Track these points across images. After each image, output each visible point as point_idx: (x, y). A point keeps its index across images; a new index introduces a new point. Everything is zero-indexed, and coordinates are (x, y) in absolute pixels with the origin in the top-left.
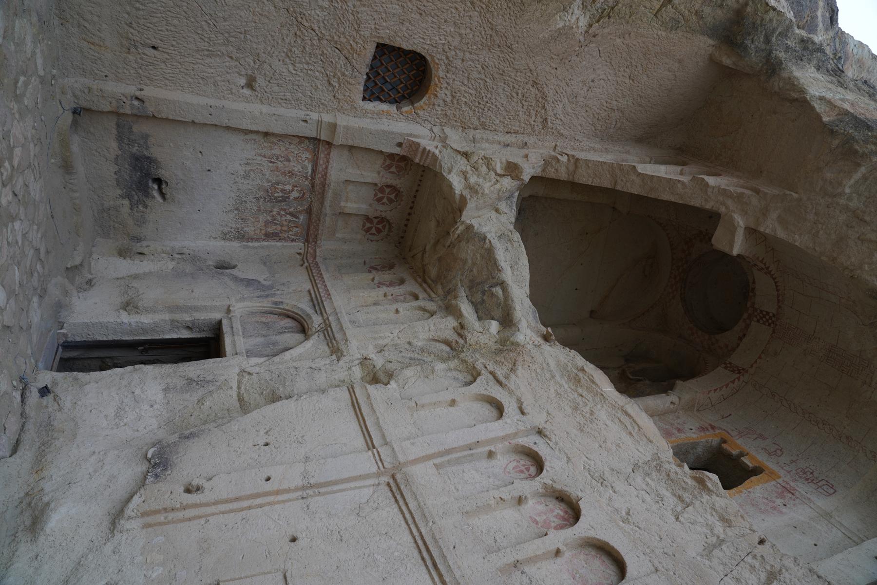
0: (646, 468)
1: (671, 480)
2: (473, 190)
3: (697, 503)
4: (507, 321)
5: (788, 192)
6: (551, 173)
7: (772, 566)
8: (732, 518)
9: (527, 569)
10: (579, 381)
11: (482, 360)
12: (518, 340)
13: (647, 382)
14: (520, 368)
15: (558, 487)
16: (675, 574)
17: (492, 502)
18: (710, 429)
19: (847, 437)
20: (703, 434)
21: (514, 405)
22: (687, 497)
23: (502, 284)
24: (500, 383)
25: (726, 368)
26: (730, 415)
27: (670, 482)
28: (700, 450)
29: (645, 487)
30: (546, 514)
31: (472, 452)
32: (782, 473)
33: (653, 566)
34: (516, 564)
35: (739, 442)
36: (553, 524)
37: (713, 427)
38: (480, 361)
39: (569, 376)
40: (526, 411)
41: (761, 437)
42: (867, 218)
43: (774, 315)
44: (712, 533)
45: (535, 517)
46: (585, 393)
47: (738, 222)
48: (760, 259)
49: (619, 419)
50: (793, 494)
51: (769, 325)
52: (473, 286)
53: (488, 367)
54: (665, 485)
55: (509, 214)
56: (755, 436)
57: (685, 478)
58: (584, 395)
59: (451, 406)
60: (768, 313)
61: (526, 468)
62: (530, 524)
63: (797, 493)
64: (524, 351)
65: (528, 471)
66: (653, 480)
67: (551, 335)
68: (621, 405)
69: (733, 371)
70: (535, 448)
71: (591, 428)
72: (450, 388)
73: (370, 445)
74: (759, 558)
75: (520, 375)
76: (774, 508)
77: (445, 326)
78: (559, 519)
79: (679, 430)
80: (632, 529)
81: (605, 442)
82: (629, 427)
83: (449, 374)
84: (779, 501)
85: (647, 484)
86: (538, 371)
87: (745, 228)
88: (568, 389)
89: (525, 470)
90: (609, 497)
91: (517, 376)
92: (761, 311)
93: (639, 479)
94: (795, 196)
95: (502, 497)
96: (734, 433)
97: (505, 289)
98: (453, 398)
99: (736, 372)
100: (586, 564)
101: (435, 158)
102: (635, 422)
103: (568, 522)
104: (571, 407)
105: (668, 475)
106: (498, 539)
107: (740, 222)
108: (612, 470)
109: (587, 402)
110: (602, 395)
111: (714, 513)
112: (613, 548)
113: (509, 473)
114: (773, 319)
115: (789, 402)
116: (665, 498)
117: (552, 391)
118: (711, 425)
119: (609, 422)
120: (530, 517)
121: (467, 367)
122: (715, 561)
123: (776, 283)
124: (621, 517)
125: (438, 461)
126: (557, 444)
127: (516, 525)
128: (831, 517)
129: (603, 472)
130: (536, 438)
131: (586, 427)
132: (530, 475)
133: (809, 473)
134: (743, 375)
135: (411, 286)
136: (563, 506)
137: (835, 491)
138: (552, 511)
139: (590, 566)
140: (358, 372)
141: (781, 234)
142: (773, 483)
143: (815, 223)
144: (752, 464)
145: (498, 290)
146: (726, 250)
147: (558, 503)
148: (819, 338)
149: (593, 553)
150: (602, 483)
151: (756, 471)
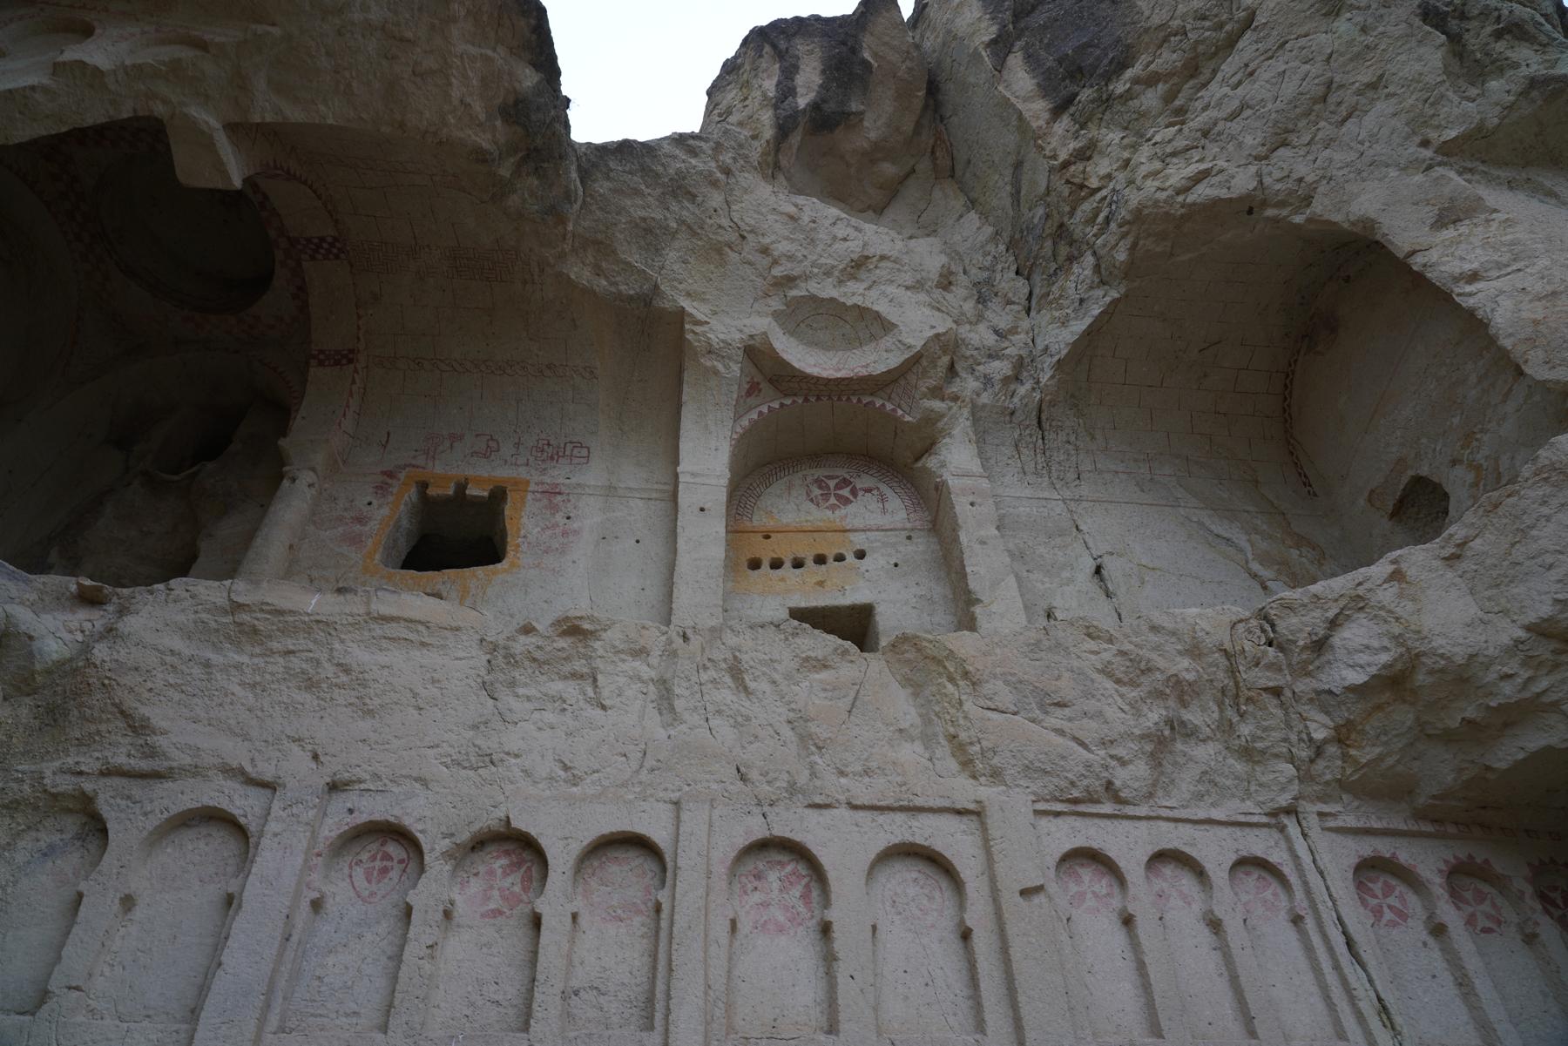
0: (501, 677)
1: (544, 663)
3: (599, 663)
5: (260, 29)
7: (725, 660)
8: (642, 642)
9: (575, 983)
10: (255, 631)
11: (48, 768)
12: (55, 657)
13: (210, 466)
14: (145, 711)
15: (464, 836)
16: (689, 785)
17: (427, 967)
18: (390, 481)
19: (549, 367)
20: (391, 499)
21: (232, 786)
22: (579, 665)
24: (157, 776)
25: (321, 364)
26: (388, 434)
27: (546, 667)
28: (405, 523)
29: (528, 706)
30: (491, 888)
31: (294, 939)
32: (523, 473)
33: (665, 802)
35: (439, 469)
36: (517, 889)
37: (390, 474)
38: (48, 773)
39: (228, 637)
40: (268, 777)
41: (455, 438)
42: (409, 35)
43: (336, 239)
44: (643, 682)
45: (486, 908)
46: (290, 644)
47: (207, 123)
48: (272, 164)
49: (385, 638)
50: (560, 493)
51: (337, 257)
53: (83, 768)
54: (544, 677)
56: (447, 444)
57: (555, 645)
58: (291, 647)
59: (129, 910)
60: (322, 239)
61: (382, 860)
62: (494, 925)
63: (563, 488)
64: (109, 674)
65: (390, 858)
66: (526, 685)
67: (99, 589)
68: (362, 611)
69: (337, 363)
70: (361, 818)
71: (376, 695)
72: (83, 887)
74: (709, 664)
75: (164, 724)
76: (565, 534)
78: (512, 871)
79: (360, 520)
80: (593, 783)
81: (415, 695)
82: (411, 636)
83: (20, 858)
84: (559, 518)
85: (529, 699)
86: (171, 681)
87: (223, 127)
88: (256, 660)
89: (385, 863)
90: (522, 771)
91: (164, 733)
92: (309, 240)
93: (508, 700)
94: (276, 31)
95: (431, 943)
96: (420, 461)
98: (118, 895)
99: (344, 361)
100: (607, 886)
102: (411, 621)
103: (526, 862)
104: (299, 688)
105: (535, 660)
106: (496, 998)
107: (209, 120)
108: (475, 727)
109: (311, 655)
110: (318, 622)
111: (623, 656)
112: (612, 833)
113: (373, 894)
114: (338, 245)
115: (447, 362)
116: (564, 695)
117: (237, 689)
118: (384, 473)
119: (382, 658)
120: (482, 916)
121: (36, 808)
122: (686, 716)
123: (310, 187)
124: (565, 781)
125: (273, 1021)
126: (377, 777)
127: (485, 950)
128: (615, 488)
129: (475, 746)
130: (340, 802)
131: (368, 701)
132: (401, 861)
133: (546, 447)
134: (357, 361)
136: (492, 848)
137: (588, 448)
138: (491, 873)
139: (613, 884)
141: (295, 115)
142: (530, 497)
143: (336, 72)
144: (484, 490)
146: (220, 186)
147: (481, 853)
148: (428, 246)
149: (596, 864)
150: (492, 762)
151: (498, 496)
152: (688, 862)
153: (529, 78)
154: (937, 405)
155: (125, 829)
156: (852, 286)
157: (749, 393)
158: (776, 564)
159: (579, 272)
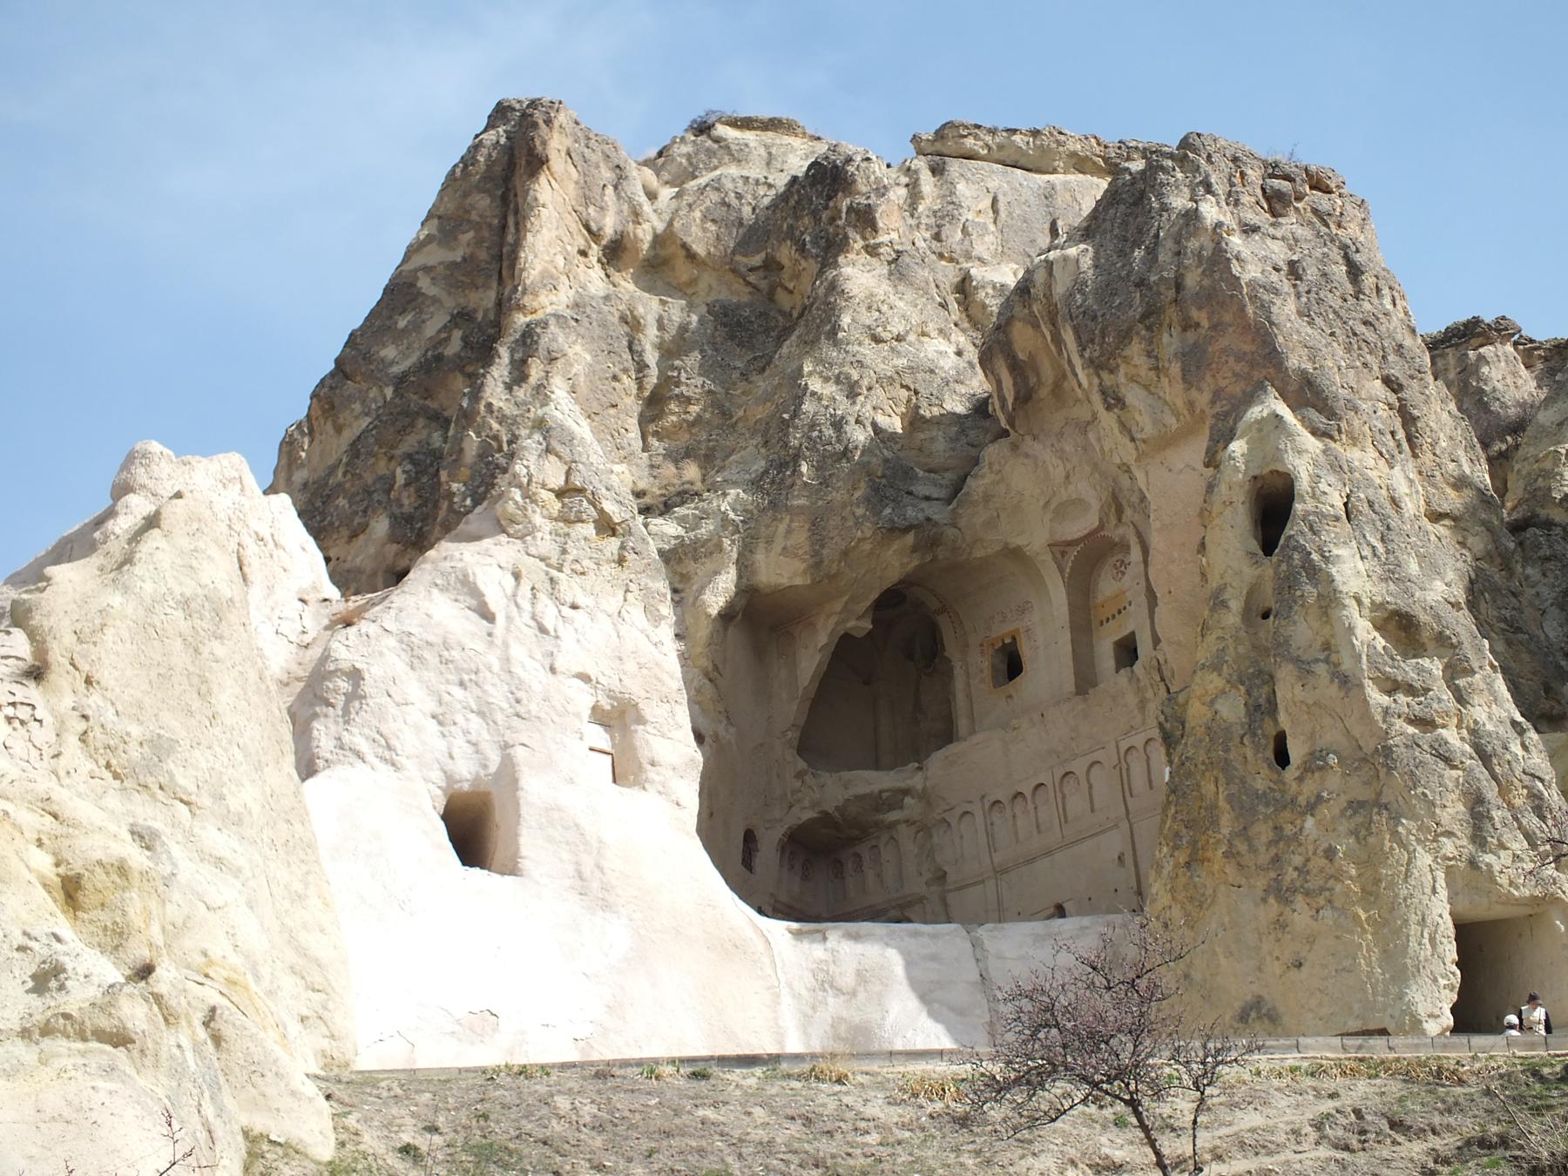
2: (814, 805)
4: (906, 792)
6: (796, 743)
23: (880, 792)
34: (1038, 826)
37: (982, 645)
52: (877, 810)
55: (827, 778)
73: (982, 882)
77: (904, 832)
97: (884, 791)
101: (790, 828)
107: (851, 624)
130: (986, 800)
135: (864, 849)
140: (934, 888)
141: (868, 603)
145: (885, 795)
151: (1014, 638)
152: (1050, 786)
153: (910, 539)
154: (1121, 530)
155: (954, 824)
156: (1071, 488)
157: (1063, 556)
158: (1108, 620)
159: (979, 553)
